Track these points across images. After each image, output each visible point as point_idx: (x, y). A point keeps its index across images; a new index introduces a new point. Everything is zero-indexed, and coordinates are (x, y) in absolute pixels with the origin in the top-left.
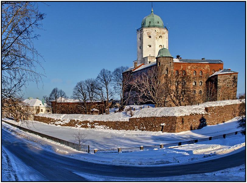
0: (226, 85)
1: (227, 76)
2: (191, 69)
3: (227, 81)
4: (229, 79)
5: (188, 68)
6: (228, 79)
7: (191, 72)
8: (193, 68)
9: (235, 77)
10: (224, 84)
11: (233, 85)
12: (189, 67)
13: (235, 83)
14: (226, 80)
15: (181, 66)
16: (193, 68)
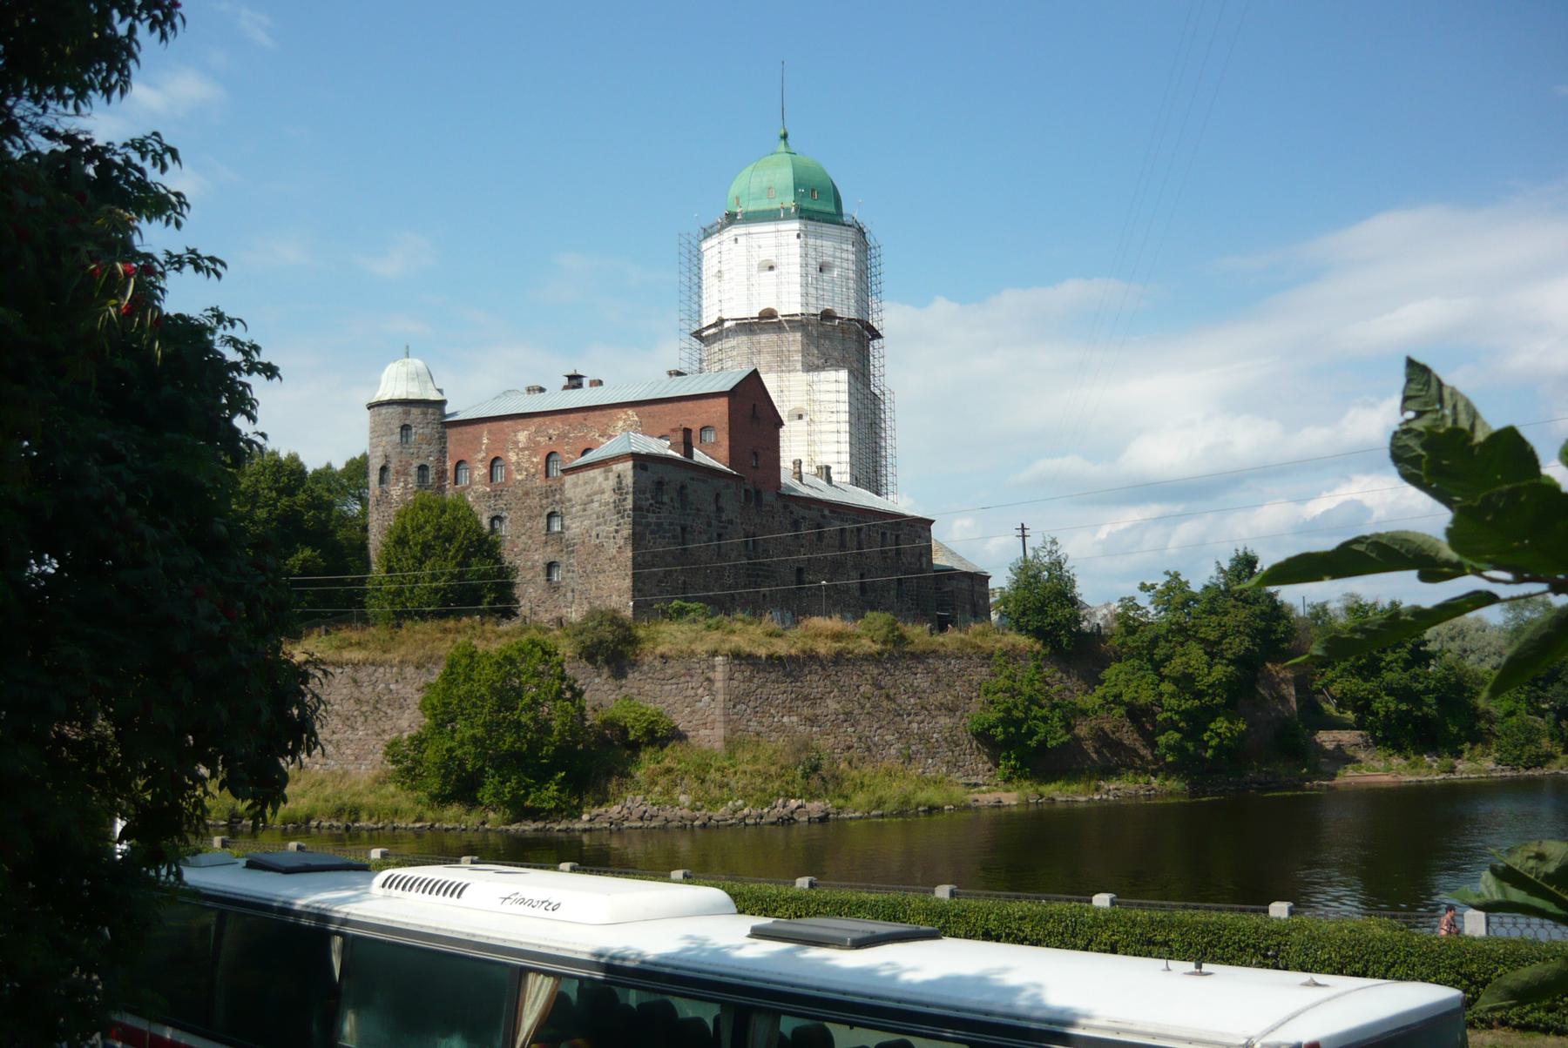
0: (594, 533)
1: (594, 479)
2: (533, 447)
3: (596, 505)
4: (603, 492)
5: (516, 443)
6: (595, 493)
7: (535, 460)
8: (542, 440)
9: (624, 482)
10: (587, 523)
11: (617, 531)
12: (522, 437)
13: (623, 517)
14: (592, 501)
15: (479, 439)
16: (542, 440)
